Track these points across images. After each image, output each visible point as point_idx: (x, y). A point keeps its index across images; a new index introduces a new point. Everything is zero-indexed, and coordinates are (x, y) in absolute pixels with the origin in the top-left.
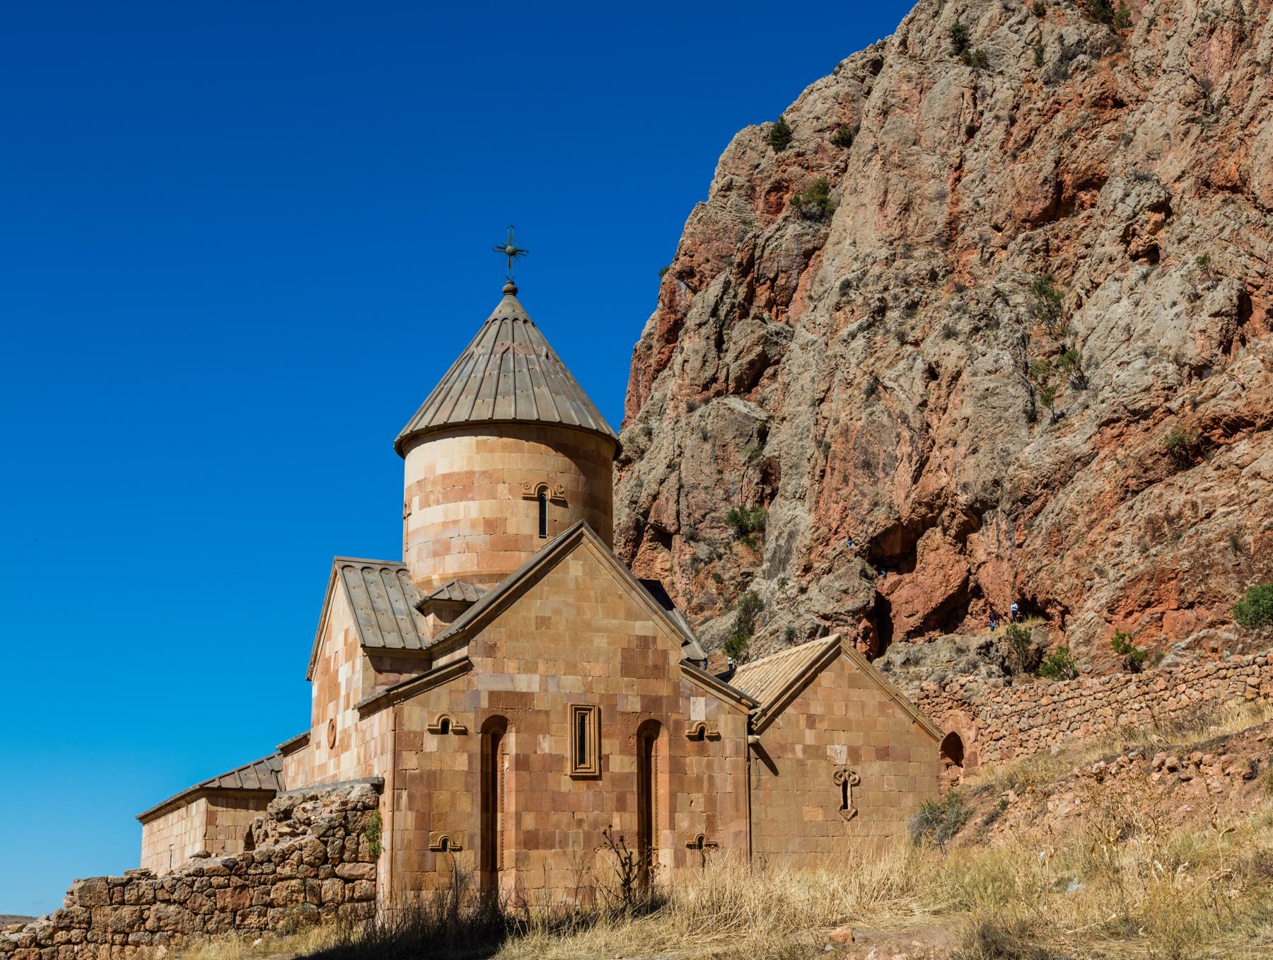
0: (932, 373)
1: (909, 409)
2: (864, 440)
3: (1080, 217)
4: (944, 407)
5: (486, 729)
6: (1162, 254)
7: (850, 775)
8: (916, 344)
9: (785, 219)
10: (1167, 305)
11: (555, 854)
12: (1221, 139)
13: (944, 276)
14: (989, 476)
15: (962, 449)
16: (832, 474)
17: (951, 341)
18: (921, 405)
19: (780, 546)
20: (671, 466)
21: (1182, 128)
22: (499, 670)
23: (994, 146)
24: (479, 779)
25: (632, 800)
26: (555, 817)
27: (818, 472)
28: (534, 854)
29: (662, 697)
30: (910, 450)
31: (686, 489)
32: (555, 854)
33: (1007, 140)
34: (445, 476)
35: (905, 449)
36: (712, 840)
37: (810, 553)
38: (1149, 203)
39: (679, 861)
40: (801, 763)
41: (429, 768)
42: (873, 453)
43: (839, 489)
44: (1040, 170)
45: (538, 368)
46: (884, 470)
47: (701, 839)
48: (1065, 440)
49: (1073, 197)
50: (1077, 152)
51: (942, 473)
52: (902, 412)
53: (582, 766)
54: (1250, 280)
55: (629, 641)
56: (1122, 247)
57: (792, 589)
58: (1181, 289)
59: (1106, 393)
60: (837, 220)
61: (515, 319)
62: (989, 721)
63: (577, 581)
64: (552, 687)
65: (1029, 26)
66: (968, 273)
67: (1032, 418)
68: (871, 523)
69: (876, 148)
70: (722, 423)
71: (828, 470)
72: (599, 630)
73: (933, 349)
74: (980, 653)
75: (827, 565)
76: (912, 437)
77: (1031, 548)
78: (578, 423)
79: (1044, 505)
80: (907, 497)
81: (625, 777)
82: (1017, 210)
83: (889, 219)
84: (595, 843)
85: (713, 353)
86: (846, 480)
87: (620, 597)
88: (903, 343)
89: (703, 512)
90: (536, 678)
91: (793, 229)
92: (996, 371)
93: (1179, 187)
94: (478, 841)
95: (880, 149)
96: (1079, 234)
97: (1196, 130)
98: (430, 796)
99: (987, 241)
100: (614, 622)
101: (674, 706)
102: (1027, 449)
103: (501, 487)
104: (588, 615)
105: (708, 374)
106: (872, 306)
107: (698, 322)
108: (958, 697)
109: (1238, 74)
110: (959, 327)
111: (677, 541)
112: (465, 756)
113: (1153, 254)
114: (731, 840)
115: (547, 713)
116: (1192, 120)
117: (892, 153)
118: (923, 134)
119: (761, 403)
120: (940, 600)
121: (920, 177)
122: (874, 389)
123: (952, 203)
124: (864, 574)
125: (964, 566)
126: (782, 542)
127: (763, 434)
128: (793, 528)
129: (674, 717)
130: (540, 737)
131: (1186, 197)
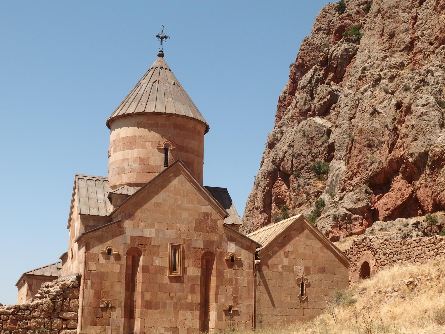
0: (398, 106)
2: (369, 135)
4: (403, 120)
5: (128, 254)
7: (305, 280)
8: (392, 93)
9: (342, 42)
11: (160, 312)
13: (407, 65)
14: (422, 150)
15: (410, 139)
16: (355, 149)
17: (408, 93)
19: (333, 180)
20: (289, 146)
22: (136, 226)
23: (431, 8)
24: (125, 276)
25: (198, 289)
26: (160, 295)
27: (349, 148)
28: (150, 311)
29: (214, 241)
32: (160, 312)
33: (437, 5)
34: (124, 138)
35: (386, 138)
36: (236, 308)
37: (345, 183)
39: (219, 318)
40: (281, 274)
41: (101, 270)
42: (372, 140)
43: (357, 156)
45: (168, 90)
46: (377, 147)
47: (230, 308)
52: (385, 122)
53: (175, 272)
55: (199, 215)
57: (337, 198)
60: (362, 41)
61: (162, 68)
62: (381, 257)
63: (175, 186)
64: (161, 235)
66: (418, 63)
68: (371, 170)
69: (379, 11)
70: (311, 128)
71: (353, 148)
72: (185, 209)
73: (399, 96)
74: (414, 227)
75: (351, 188)
76: (389, 133)
77: (439, 182)
78: (184, 115)
80: (386, 159)
81: (195, 278)
82: (441, 36)
83: (384, 40)
84: (179, 307)
85: (309, 98)
86: (360, 152)
87: (196, 194)
88: (387, 93)
89: (302, 165)
90: (154, 230)
91: (345, 46)
92: (427, 105)
94: (123, 304)
95: (381, 10)
98: (101, 283)
100: (192, 205)
101: (220, 244)
102: (439, 139)
103: (148, 143)
104: (179, 202)
105: (307, 107)
106: (375, 77)
107: (303, 85)
108: (368, 245)
110: (411, 86)
111: (291, 178)
112: (119, 265)
114: (245, 308)
115: (158, 247)
117: (386, 12)
118: (400, 4)
119: (329, 120)
120: (400, 204)
121: (398, 22)
122: (375, 112)
123: (412, 33)
124: (366, 192)
125: (411, 189)
126: (334, 178)
128: (339, 172)
129: (219, 250)
130: (155, 258)
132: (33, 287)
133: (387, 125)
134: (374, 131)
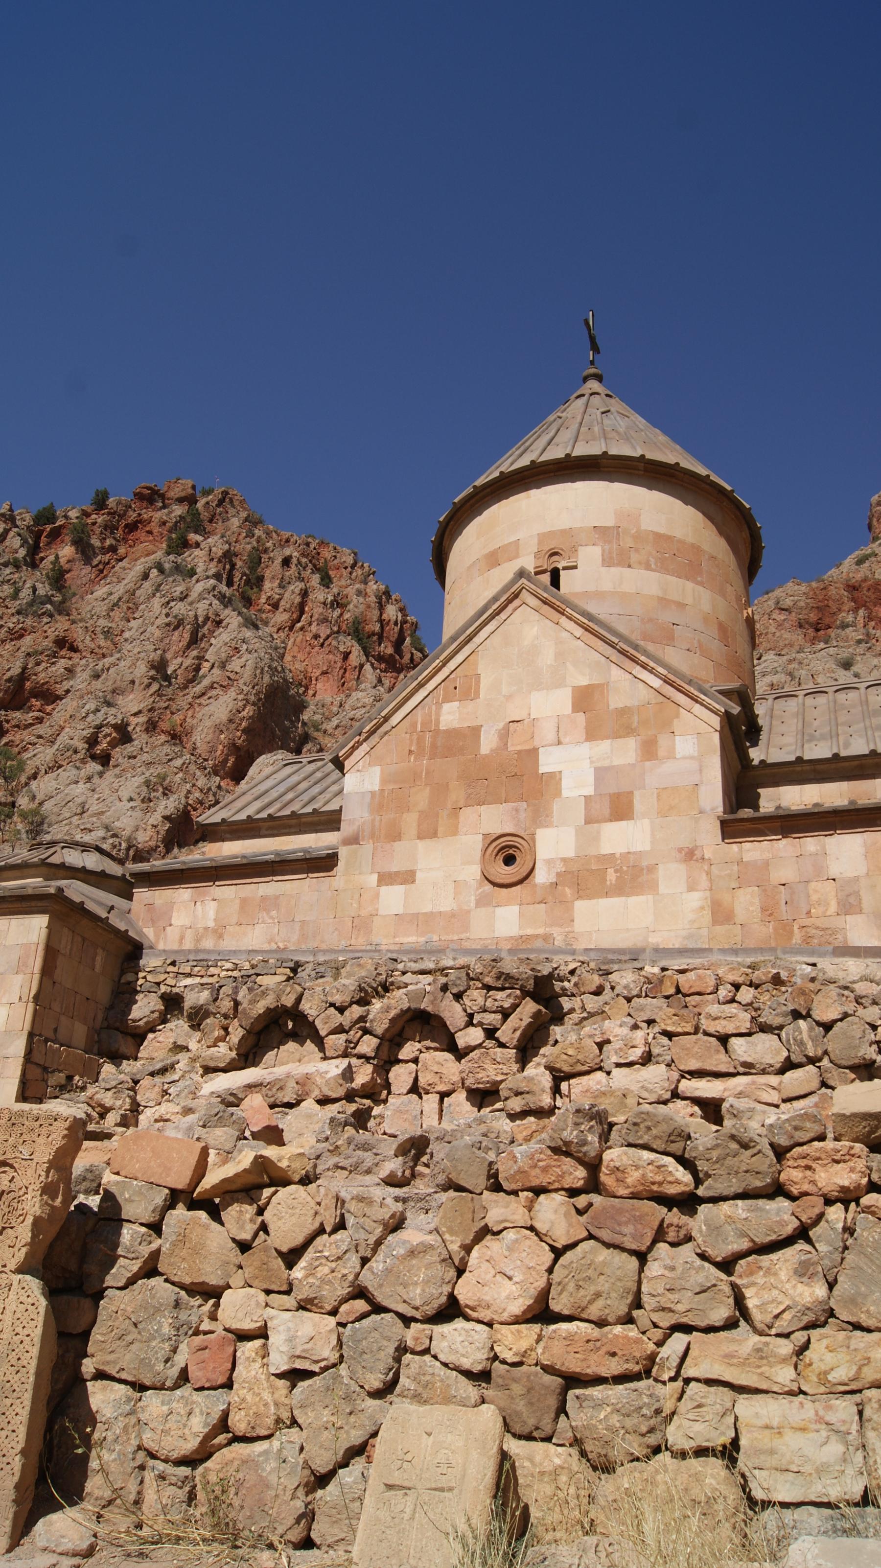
3: (31, 714)
10: (124, 799)
12: (169, 700)
21: (146, 681)
34: (659, 537)
38: (113, 722)
44: (9, 670)
49: (28, 700)
50: (41, 668)
54: (191, 802)
56: (86, 746)
58: (138, 790)
65: (8, 571)
93: (134, 721)
96: (27, 726)
97: (155, 687)
109: (188, 662)
113: (105, 760)
116: (153, 678)
131: (138, 729)
132: (61, 961)
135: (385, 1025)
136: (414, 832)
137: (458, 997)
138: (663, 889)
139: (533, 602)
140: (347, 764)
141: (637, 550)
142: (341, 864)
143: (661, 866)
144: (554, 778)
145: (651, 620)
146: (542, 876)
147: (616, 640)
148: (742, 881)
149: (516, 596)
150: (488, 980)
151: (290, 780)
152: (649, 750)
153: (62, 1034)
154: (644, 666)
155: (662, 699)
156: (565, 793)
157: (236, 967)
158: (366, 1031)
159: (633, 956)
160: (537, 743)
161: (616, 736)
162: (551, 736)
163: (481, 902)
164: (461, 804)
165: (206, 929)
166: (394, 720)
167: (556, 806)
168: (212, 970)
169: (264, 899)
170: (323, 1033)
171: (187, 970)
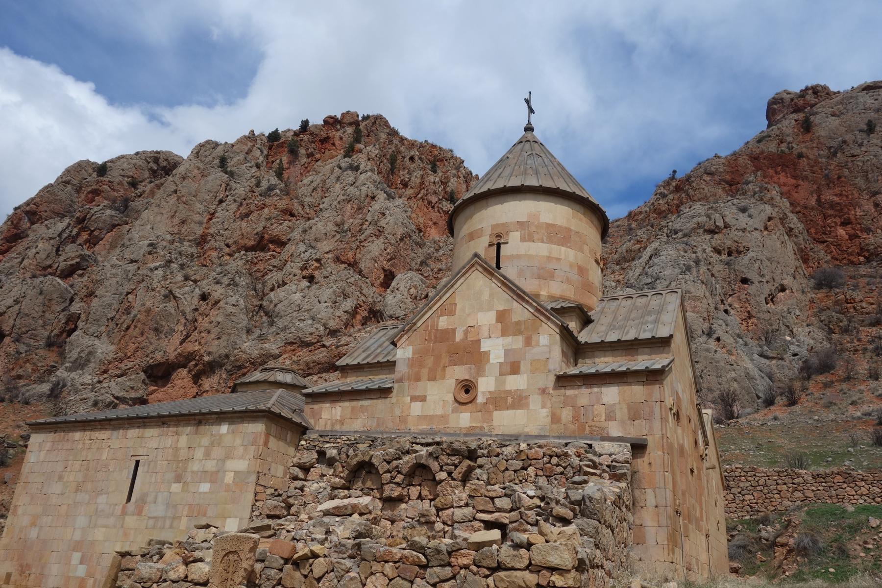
0: (204, 297)
1: (188, 310)
3: (269, 253)
6: (315, 280)
8: (195, 282)
14: (223, 351)
15: (213, 336)
17: (219, 285)
18: (194, 310)
30: (183, 329)
31: (22, 315)
35: (181, 328)
48: (266, 345)
49: (267, 245)
51: (197, 344)
52: (183, 310)
59: (293, 330)
67: (249, 331)
73: (206, 286)
79: (248, 371)
96: (267, 261)
99: (221, 249)
102: (245, 344)
127: (72, 300)
133: (185, 313)
134: (168, 316)
135: (407, 469)
136: (426, 377)
137: (437, 458)
138: (531, 407)
139: (480, 269)
140: (398, 345)
141: (537, 233)
142: (395, 391)
143: (531, 397)
144: (487, 353)
145: (542, 268)
146: (480, 399)
147: (515, 289)
148: (565, 404)
149: (473, 266)
150: (448, 451)
151: (381, 340)
152: (528, 342)
153: (273, 472)
154: (527, 302)
155: (534, 317)
156: (491, 361)
157: (348, 440)
158: (399, 472)
159: (516, 438)
160: (480, 337)
161: (514, 334)
162: (486, 334)
163: (453, 412)
164: (447, 365)
165: (336, 420)
166: (419, 324)
167: (487, 367)
168: (339, 440)
169: (362, 407)
170: (381, 473)
171: (328, 440)
